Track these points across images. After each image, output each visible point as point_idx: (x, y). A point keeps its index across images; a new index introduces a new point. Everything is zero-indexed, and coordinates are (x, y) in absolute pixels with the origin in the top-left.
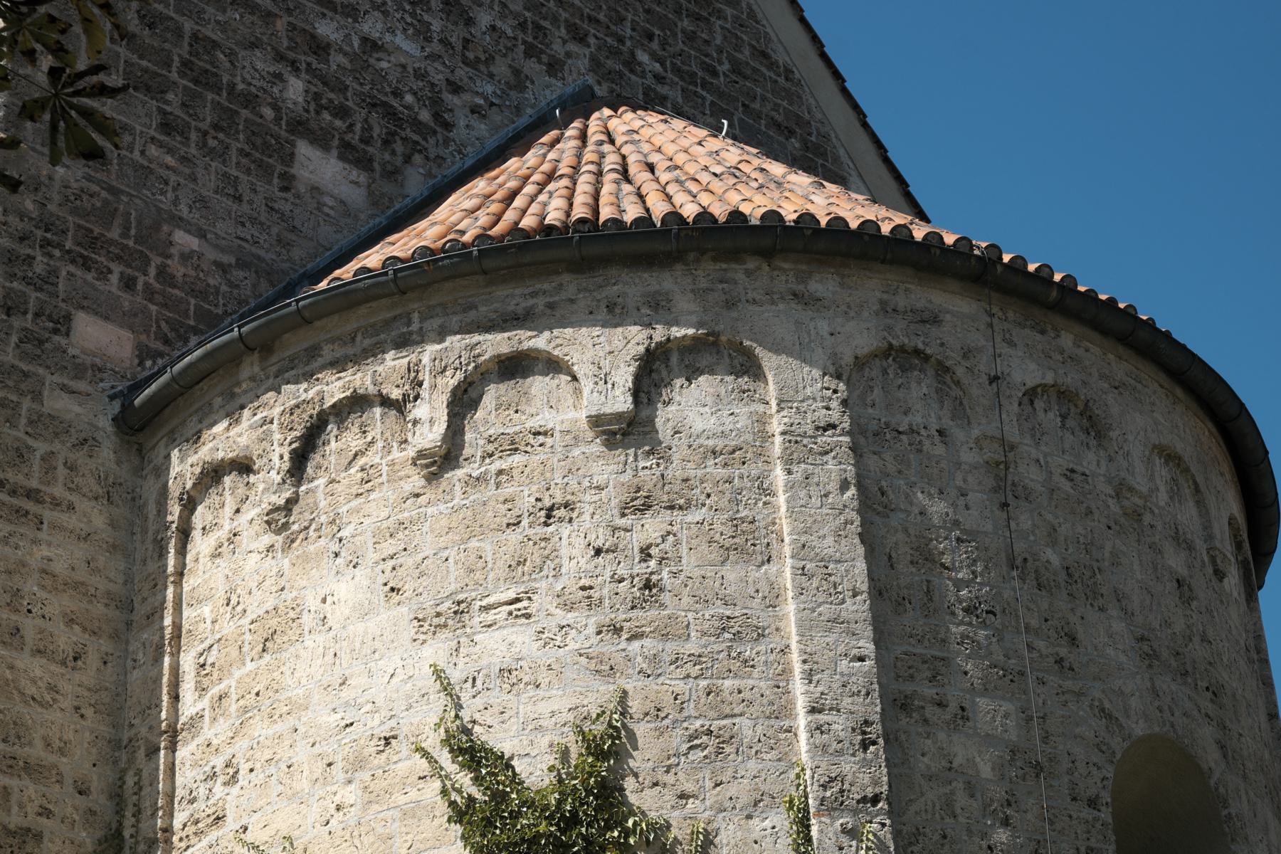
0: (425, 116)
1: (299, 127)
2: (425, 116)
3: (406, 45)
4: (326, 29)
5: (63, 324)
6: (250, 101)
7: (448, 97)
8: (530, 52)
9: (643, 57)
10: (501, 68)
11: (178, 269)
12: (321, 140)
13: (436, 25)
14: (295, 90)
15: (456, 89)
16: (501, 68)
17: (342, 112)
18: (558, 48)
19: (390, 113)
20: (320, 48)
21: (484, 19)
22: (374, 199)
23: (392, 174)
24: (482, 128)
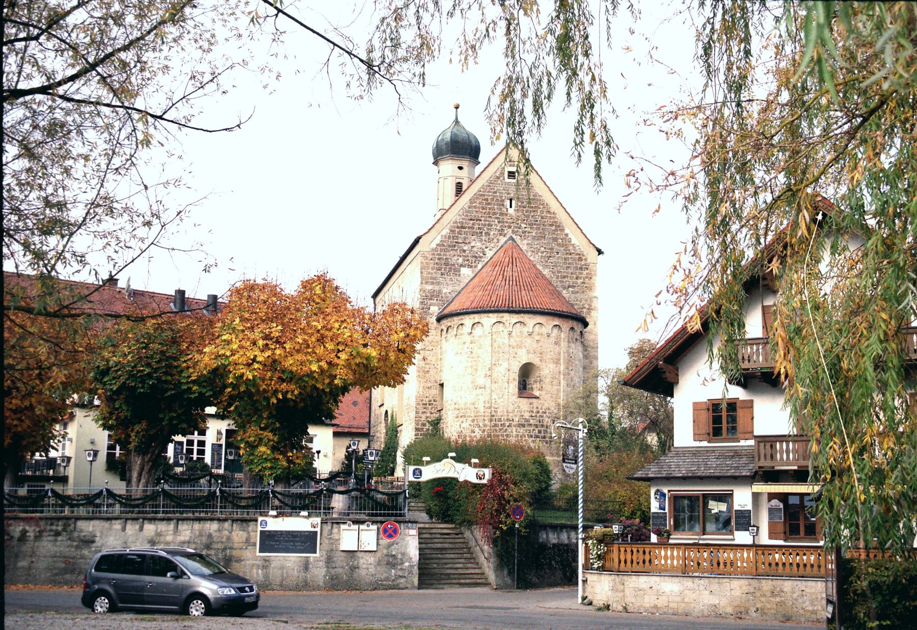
0: (481, 255)
1: (461, 266)
2: (481, 255)
3: (479, 244)
4: (465, 248)
5: (429, 309)
6: (454, 265)
7: (486, 250)
8: (501, 235)
9: (523, 226)
10: (495, 240)
11: (443, 295)
12: (464, 266)
13: (484, 238)
14: (460, 260)
15: (487, 248)
16: (495, 240)
17: (468, 260)
18: (506, 232)
19: (476, 257)
20: (464, 251)
21: (492, 233)
22: (473, 272)
23: (476, 267)
24: (491, 252)
